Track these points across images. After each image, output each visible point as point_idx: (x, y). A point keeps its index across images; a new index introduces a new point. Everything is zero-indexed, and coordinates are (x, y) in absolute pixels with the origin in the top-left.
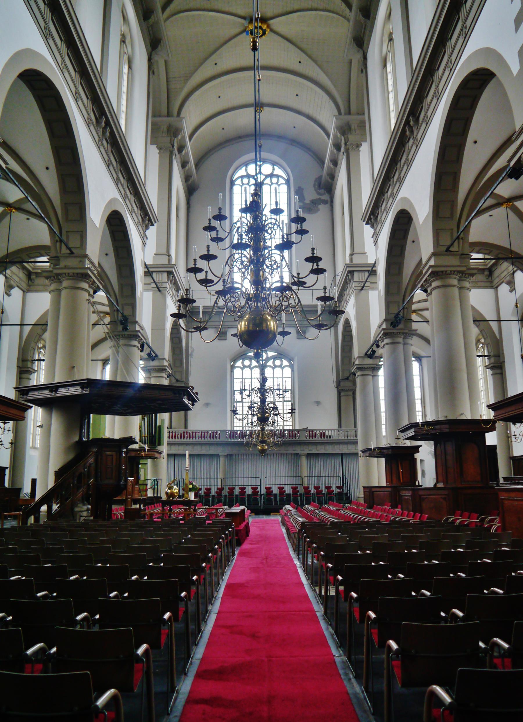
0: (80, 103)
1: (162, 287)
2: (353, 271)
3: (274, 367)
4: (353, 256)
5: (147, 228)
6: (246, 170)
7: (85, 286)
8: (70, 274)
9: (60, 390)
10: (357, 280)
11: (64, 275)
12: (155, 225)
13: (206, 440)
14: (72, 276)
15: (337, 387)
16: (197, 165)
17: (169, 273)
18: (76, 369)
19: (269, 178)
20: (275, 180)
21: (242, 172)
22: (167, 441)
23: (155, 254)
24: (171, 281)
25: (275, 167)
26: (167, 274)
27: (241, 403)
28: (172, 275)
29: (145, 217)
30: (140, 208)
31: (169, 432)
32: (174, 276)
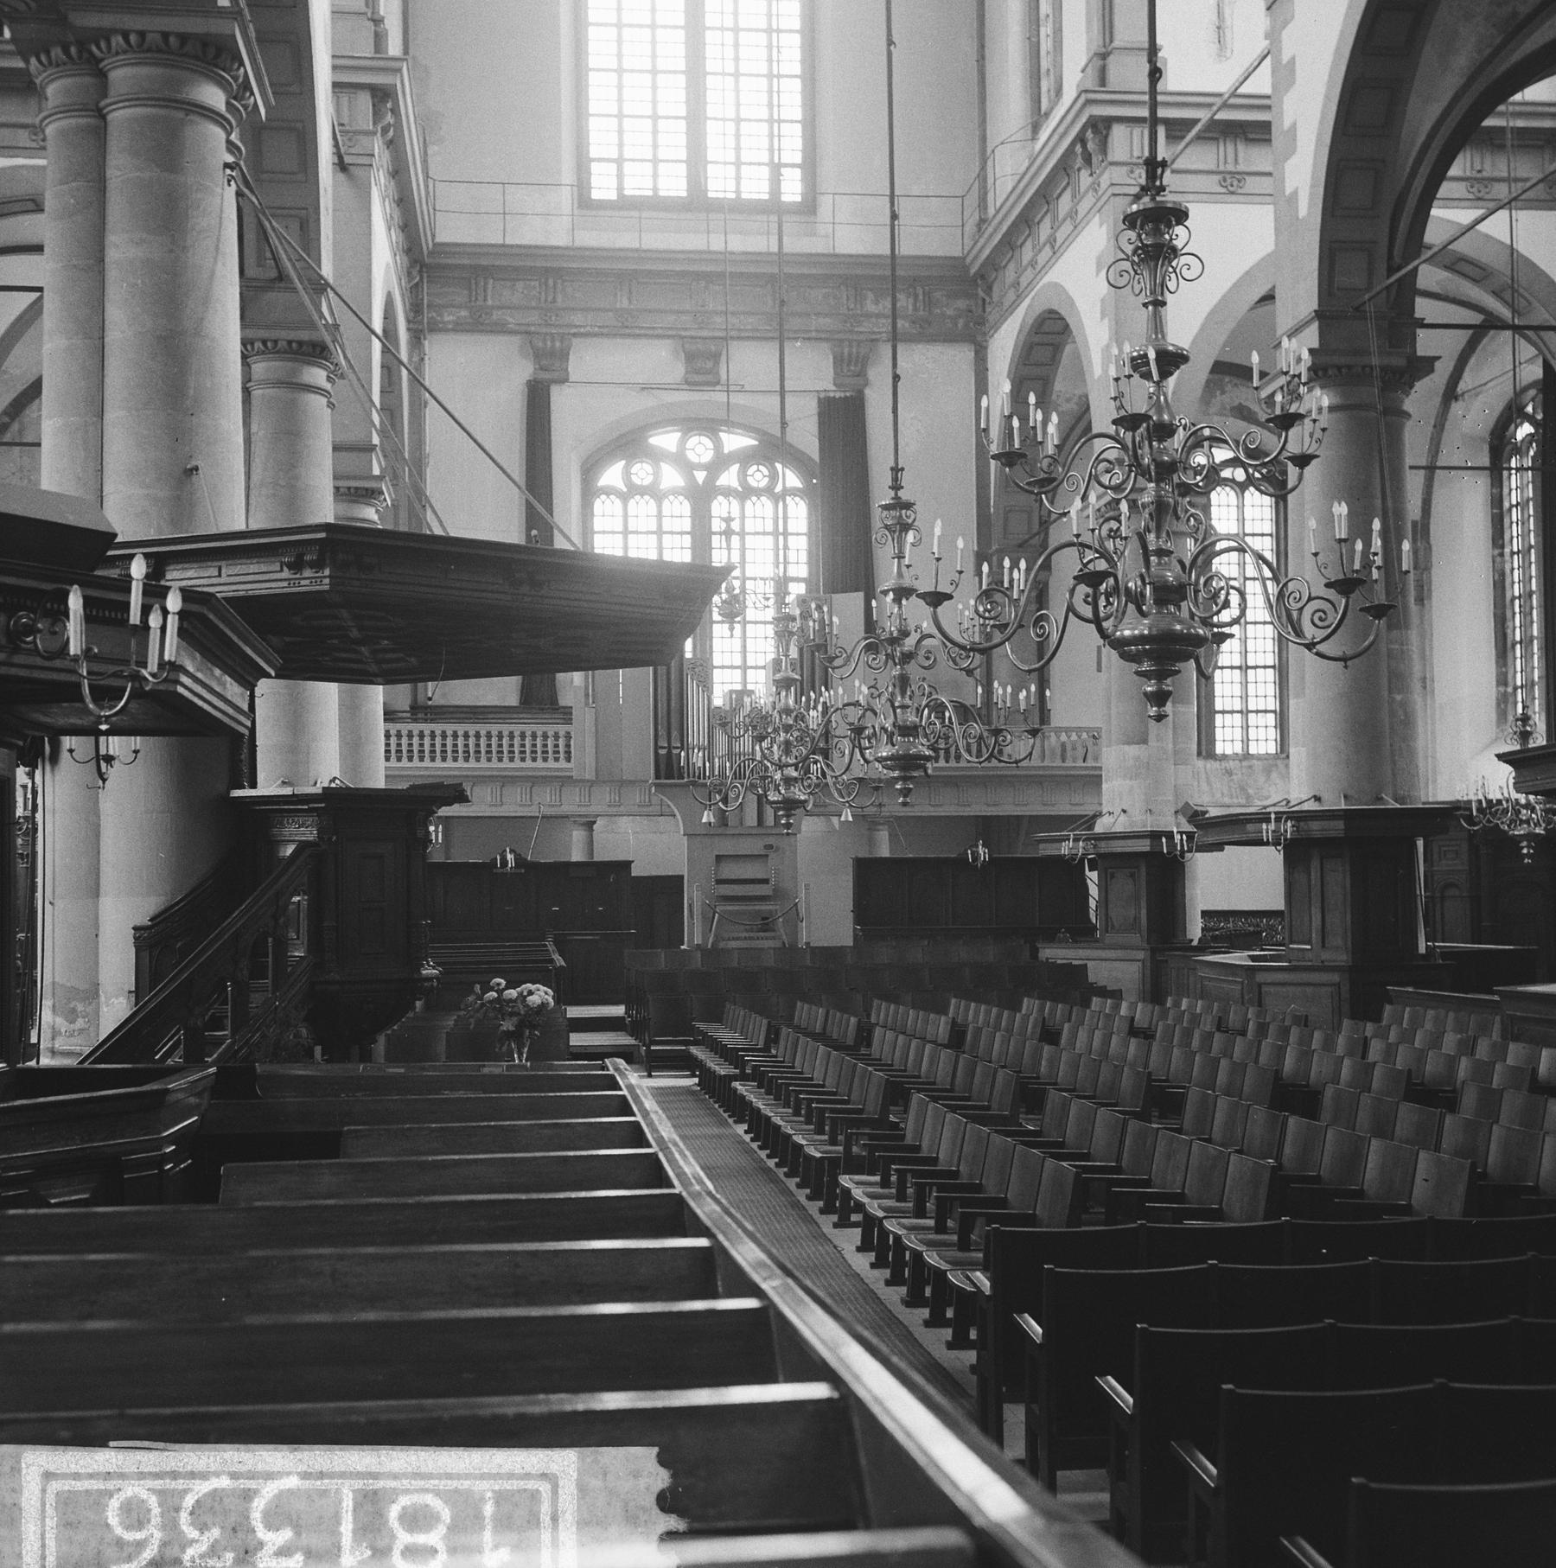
1: (353, 151)
2: (1109, 121)
4: (1111, 58)
7: (214, 97)
8: (149, 37)
11: (117, 41)
14: (159, 51)
18: (201, 480)
24: (385, 131)
26: (373, 97)
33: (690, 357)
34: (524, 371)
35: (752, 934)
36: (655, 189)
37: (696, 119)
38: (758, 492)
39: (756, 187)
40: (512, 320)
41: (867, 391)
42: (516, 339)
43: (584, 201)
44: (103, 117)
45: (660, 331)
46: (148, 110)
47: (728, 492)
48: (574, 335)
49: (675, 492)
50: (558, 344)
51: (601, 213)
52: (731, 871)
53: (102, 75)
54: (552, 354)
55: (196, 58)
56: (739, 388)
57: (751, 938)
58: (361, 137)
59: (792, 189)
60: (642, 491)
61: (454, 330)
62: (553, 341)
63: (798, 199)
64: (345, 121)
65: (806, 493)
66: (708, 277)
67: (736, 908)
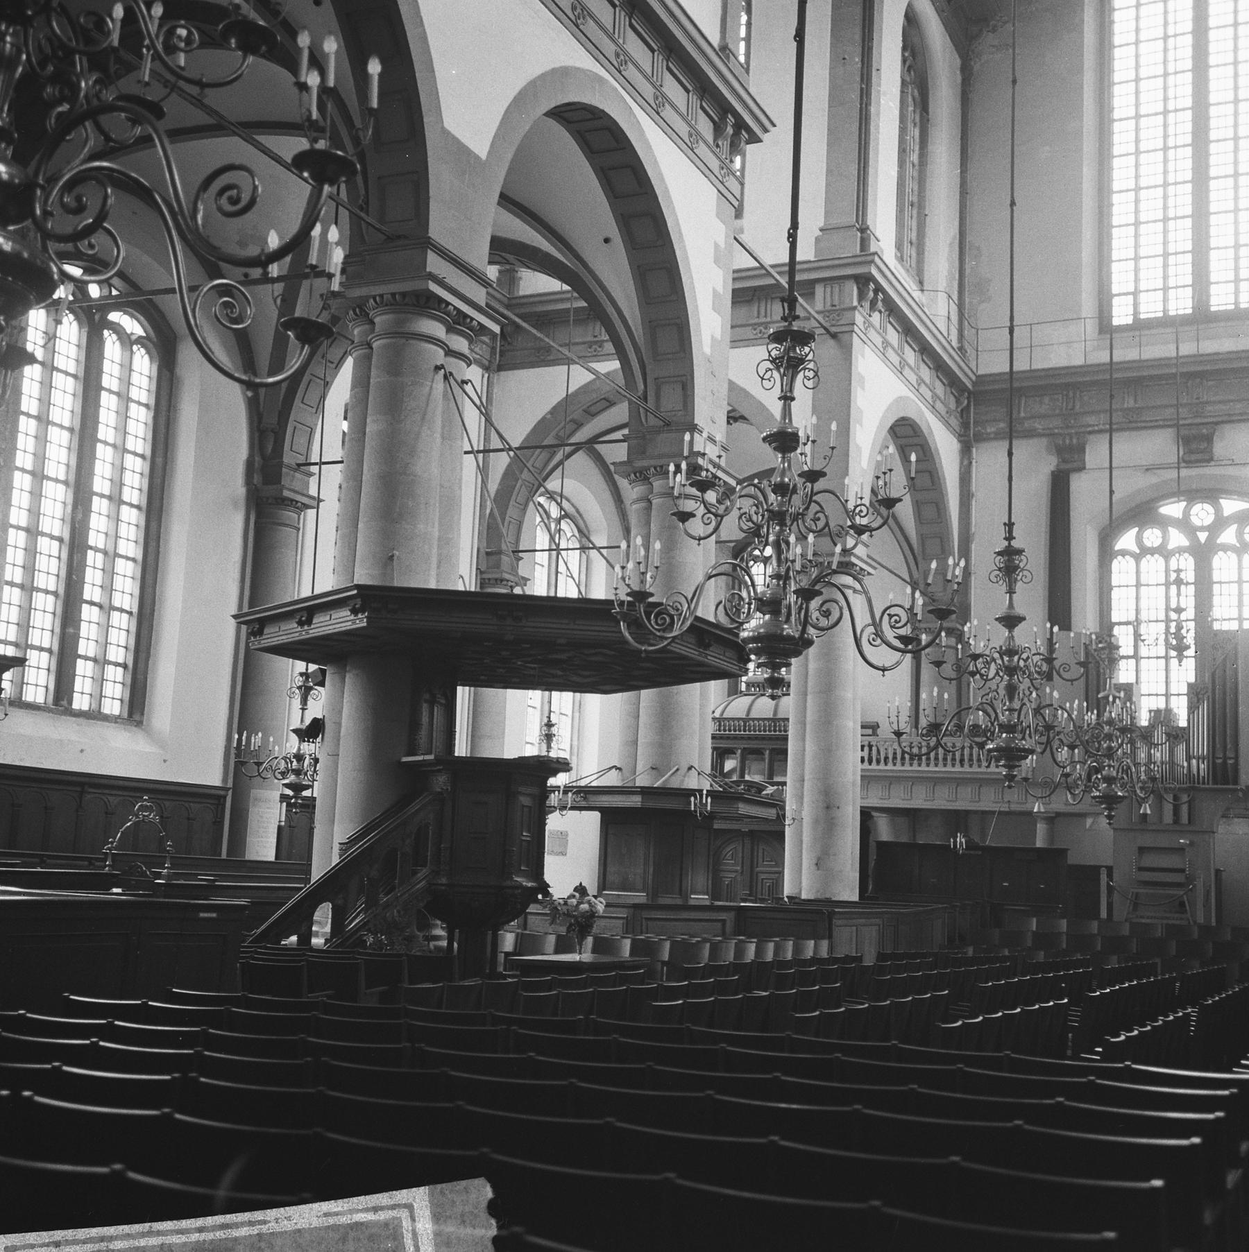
5: (735, 148)
9: (319, 619)
12: (765, 137)
13: (975, 769)
14: (391, 305)
22: (862, 770)
23: (821, 230)
26: (857, 284)
27: (1133, 661)
28: (872, 286)
29: (723, 118)
30: (695, 89)
31: (870, 747)
32: (879, 289)
34: (1049, 464)
35: (1168, 915)
36: (1236, 303)
40: (1038, 425)
42: (1044, 441)
43: (1105, 326)
44: (372, 348)
45: (1161, 423)
46: (388, 341)
47: (1225, 548)
48: (1090, 433)
49: (1180, 550)
50: (1075, 441)
51: (1154, 331)
52: (1150, 860)
53: (372, 323)
54: (1071, 449)
55: (414, 305)
56: (1230, 462)
57: (1167, 918)
58: (845, 313)
60: (1152, 551)
61: (995, 439)
62: (1071, 439)
64: (836, 302)
67: (1152, 891)
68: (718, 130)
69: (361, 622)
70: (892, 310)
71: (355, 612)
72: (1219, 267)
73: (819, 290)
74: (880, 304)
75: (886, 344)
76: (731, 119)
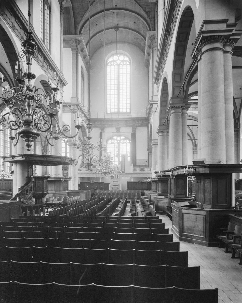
0: (16, 31)
2: (153, 103)
3: (123, 143)
5: (63, 87)
6: (113, 58)
10: (154, 107)
12: (66, 85)
15: (148, 151)
16: (91, 58)
17: (77, 105)
19: (122, 62)
20: (125, 63)
21: (110, 59)
25: (125, 57)
28: (79, 106)
32: (80, 107)
33: (117, 129)
34: (100, 131)
37: (118, 104)
38: (125, 143)
39: (125, 111)
41: (136, 132)
42: (99, 128)
43: (106, 113)
47: (121, 143)
49: (116, 143)
59: (128, 111)
60: (113, 143)
63: (129, 112)
65: (130, 143)
66: (119, 121)
68: (60, 84)
69: (24, 159)
70: (81, 110)
71: (23, 157)
72: (121, 106)
73: (71, 106)
74: (79, 109)
75: (80, 114)
76: (62, 82)
